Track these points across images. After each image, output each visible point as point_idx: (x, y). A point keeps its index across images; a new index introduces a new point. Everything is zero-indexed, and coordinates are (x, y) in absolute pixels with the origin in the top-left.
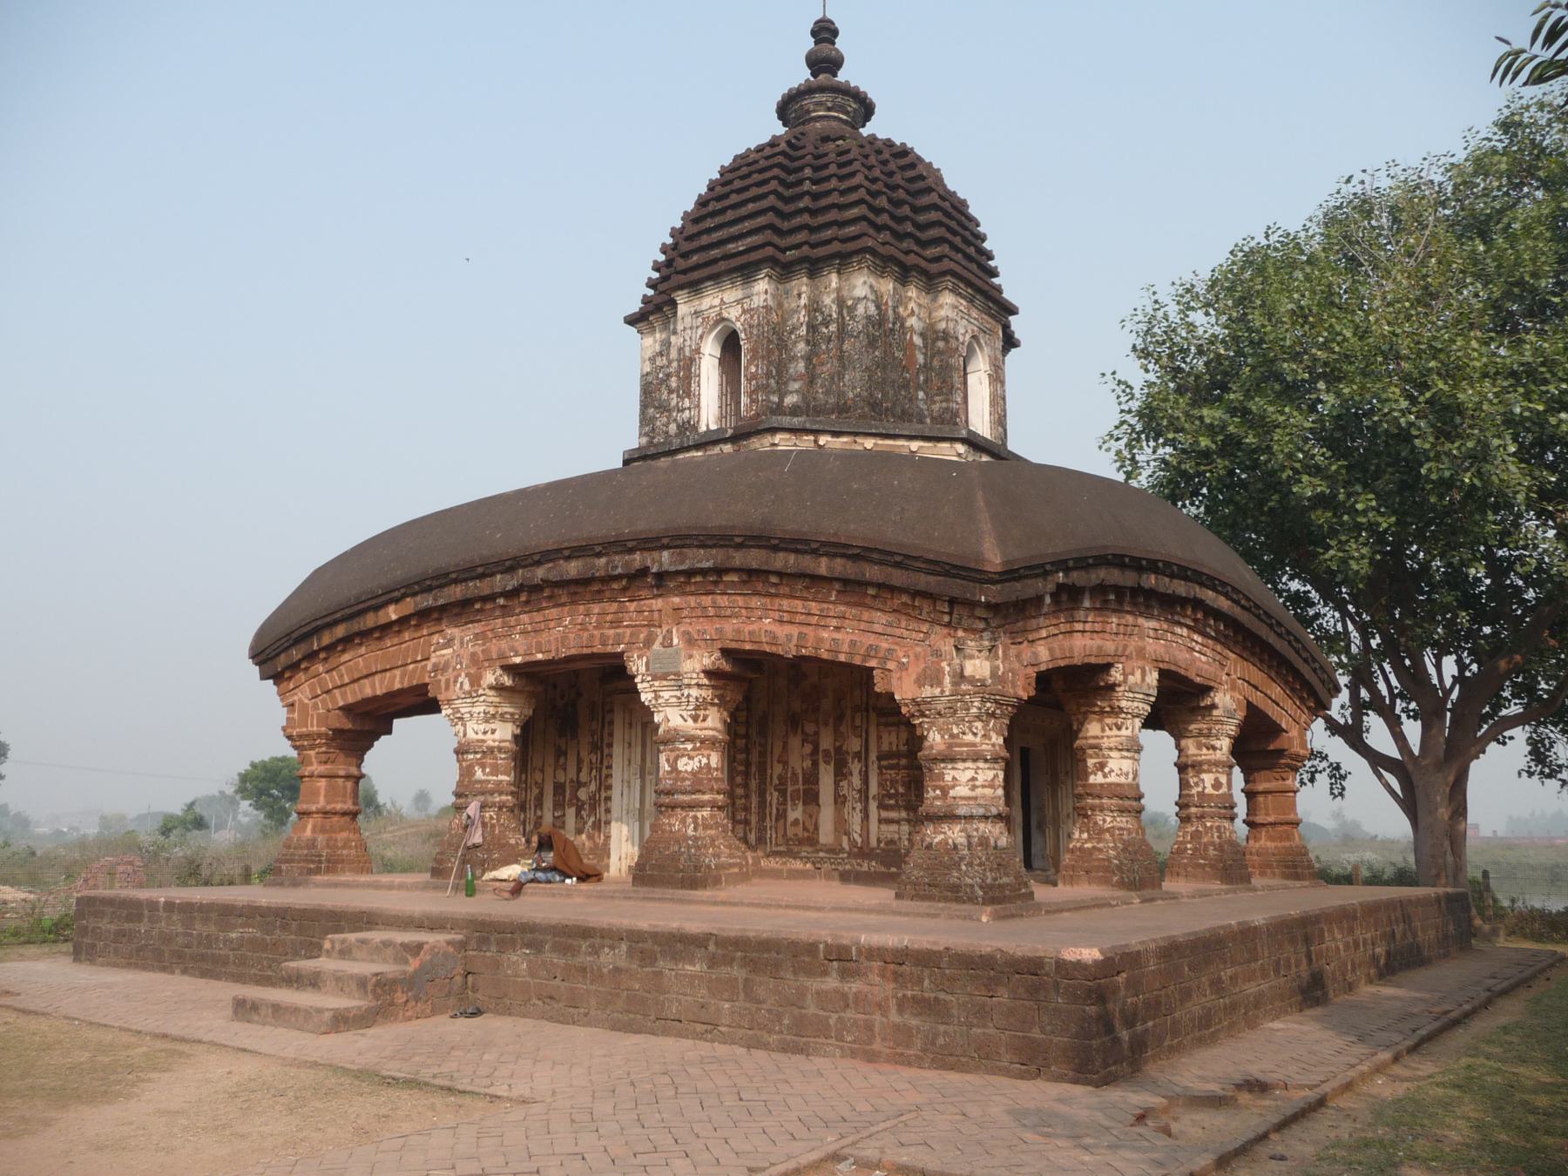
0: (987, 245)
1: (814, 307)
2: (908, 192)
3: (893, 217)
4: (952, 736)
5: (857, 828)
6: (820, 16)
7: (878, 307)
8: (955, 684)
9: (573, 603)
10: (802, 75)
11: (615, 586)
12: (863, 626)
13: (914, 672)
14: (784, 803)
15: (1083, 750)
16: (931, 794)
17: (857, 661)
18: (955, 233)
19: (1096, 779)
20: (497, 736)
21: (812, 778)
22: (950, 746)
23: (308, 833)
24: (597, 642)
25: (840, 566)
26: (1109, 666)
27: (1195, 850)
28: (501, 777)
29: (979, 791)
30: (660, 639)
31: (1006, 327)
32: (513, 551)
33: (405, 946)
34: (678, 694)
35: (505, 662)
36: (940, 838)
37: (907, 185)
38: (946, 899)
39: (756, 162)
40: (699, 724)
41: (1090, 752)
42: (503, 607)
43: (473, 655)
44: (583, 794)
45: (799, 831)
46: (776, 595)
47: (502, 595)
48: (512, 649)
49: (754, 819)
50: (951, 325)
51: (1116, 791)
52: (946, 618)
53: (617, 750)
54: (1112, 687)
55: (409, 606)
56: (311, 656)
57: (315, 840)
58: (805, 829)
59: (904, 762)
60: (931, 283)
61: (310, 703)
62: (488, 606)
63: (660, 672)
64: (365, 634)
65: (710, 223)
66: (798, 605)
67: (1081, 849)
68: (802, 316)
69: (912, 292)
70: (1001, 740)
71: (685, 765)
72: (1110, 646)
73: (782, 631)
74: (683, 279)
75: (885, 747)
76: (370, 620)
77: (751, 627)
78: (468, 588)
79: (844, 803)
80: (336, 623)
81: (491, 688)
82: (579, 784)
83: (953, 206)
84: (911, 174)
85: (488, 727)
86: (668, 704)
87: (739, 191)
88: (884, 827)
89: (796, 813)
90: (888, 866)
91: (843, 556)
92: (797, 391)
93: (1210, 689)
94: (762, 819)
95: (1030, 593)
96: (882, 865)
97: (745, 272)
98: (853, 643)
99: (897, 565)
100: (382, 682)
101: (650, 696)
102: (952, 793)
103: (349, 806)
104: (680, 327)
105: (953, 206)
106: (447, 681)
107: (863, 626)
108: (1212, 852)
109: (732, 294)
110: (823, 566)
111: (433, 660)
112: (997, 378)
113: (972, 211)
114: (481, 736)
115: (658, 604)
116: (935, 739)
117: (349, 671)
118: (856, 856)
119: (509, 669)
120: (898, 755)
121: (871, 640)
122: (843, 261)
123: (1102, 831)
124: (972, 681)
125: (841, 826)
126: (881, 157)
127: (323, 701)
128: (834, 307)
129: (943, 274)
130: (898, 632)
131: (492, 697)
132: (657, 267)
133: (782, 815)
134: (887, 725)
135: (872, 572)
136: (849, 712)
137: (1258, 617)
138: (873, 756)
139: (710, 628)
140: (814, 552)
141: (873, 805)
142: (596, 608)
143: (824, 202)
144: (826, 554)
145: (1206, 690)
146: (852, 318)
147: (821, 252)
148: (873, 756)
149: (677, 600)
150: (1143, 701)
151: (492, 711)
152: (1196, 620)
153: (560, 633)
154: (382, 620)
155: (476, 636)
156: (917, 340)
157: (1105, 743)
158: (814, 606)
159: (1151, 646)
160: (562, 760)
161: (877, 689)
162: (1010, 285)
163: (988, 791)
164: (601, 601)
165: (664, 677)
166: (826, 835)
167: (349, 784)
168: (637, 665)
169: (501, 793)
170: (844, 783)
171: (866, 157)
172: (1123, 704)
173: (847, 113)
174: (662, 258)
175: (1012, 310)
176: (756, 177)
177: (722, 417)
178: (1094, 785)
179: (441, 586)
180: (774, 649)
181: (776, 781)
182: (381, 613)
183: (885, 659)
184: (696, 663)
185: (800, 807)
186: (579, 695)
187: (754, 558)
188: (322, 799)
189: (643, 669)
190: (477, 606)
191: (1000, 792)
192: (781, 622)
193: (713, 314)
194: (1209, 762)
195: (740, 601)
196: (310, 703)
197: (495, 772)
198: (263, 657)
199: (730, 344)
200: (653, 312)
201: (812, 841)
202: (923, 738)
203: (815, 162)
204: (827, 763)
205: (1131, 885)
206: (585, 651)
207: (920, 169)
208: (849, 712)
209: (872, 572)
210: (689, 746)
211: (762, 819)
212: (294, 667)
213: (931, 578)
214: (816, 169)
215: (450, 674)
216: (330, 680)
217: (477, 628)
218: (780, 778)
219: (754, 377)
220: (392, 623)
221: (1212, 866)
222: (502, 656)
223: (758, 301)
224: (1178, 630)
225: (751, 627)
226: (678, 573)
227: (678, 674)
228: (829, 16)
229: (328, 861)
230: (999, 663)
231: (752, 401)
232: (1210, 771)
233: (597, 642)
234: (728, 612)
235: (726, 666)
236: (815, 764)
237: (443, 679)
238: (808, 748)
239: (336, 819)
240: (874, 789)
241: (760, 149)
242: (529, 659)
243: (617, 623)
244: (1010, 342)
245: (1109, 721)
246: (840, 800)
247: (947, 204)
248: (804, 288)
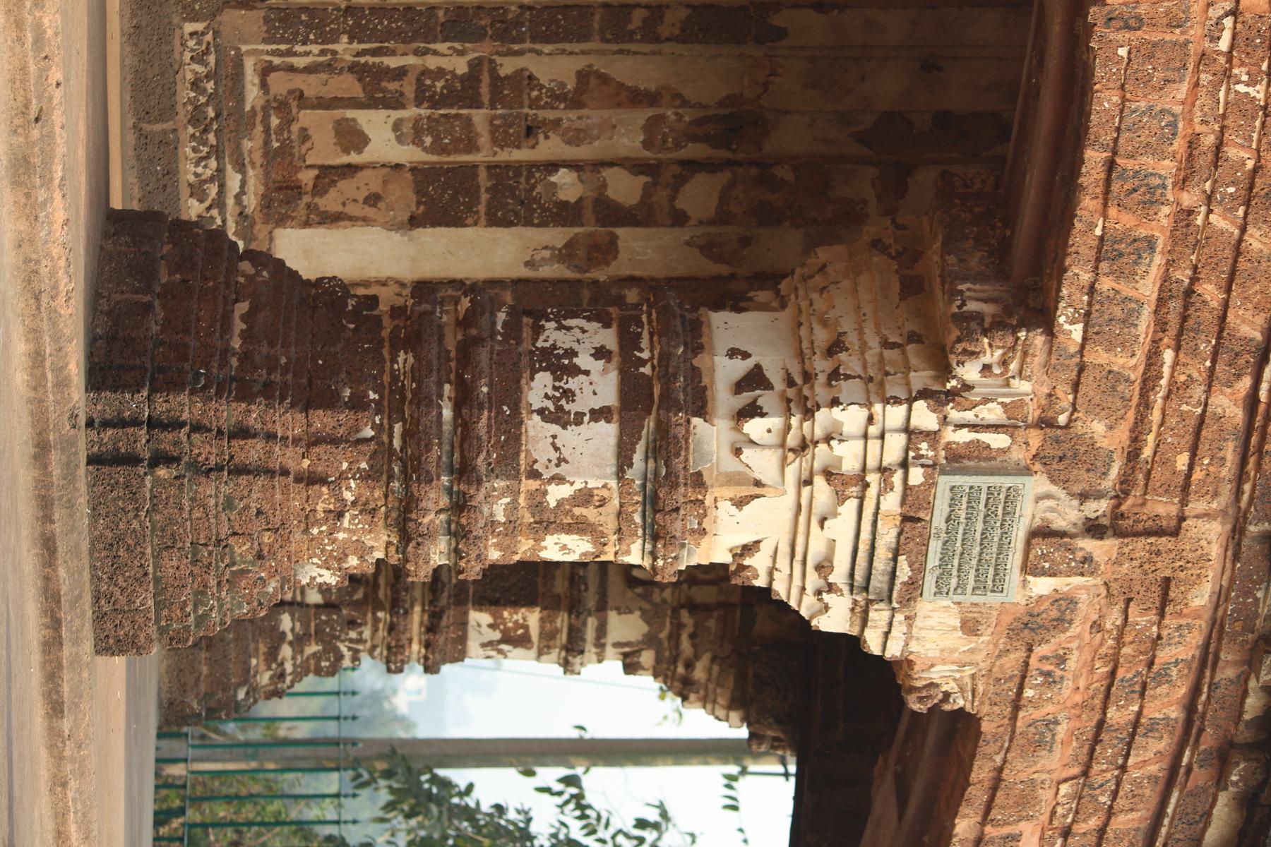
21: (512, 199)
30: (1067, 514)
34: (839, 576)
41: (562, 621)
58: (329, 175)
89: (383, 138)
101: (848, 456)
115: (1209, 535)
133: (377, 89)
139: (1061, 704)
149: (1201, 597)
178: (463, 624)
181: (507, 66)
185: (409, 154)
201: (286, 199)
204: (565, 254)
206: (1094, 158)
218: (524, 80)
234: (1103, 772)
236: (565, 214)
238: (624, 188)
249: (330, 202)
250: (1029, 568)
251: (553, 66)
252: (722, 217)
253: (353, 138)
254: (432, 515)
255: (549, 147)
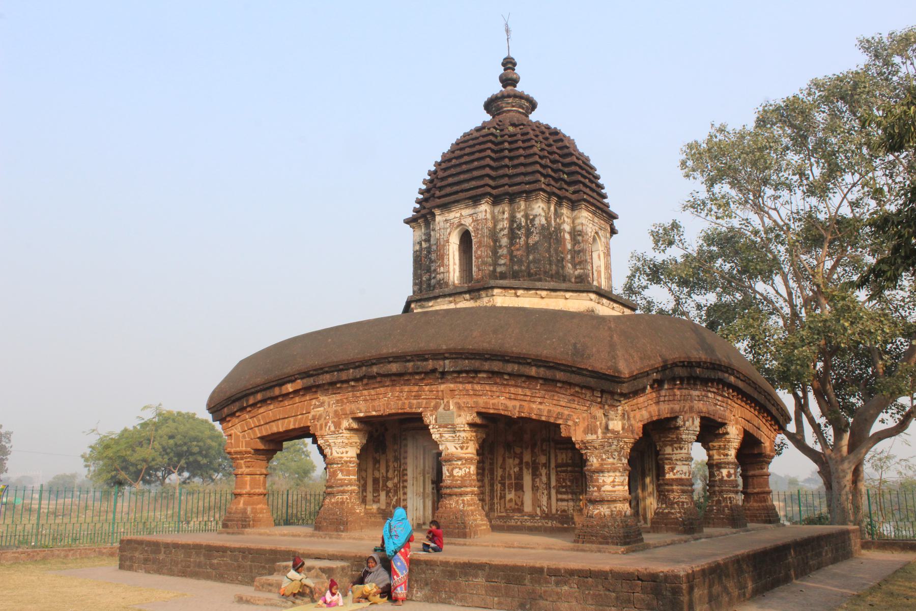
0: (600, 181)
1: (512, 219)
2: (560, 156)
3: (553, 170)
4: (602, 460)
5: (545, 503)
6: (506, 56)
7: (546, 219)
8: (603, 433)
9: (393, 385)
10: (497, 88)
11: (417, 377)
12: (555, 402)
13: (582, 426)
14: (504, 490)
15: (662, 459)
16: (592, 489)
17: (552, 420)
18: (585, 177)
19: (670, 476)
20: (349, 454)
21: (519, 477)
22: (602, 465)
23: (241, 505)
24: (407, 406)
25: (542, 372)
26: (676, 417)
27: (718, 510)
28: (351, 477)
29: (617, 488)
30: (442, 406)
31: (612, 226)
32: (360, 357)
33: (323, 570)
35: (353, 416)
36: (596, 512)
37: (558, 151)
38: (601, 543)
39: (477, 138)
40: (464, 451)
42: (353, 386)
43: (336, 412)
44: (390, 484)
45: (513, 504)
46: (507, 385)
47: (353, 380)
48: (358, 409)
49: (487, 498)
50: (584, 227)
51: (680, 482)
52: (599, 400)
53: (410, 461)
54: (678, 428)
55: (299, 384)
56: (242, 409)
57: (246, 509)
58: (516, 504)
59: (569, 469)
60: (574, 205)
61: (241, 435)
62: (345, 385)
63: (443, 424)
64: (274, 399)
65: (453, 171)
66: (520, 391)
67: (662, 513)
68: (506, 224)
69: (565, 211)
70: (626, 461)
71: (458, 473)
72: (677, 407)
73: (510, 404)
74: (438, 201)
75: (560, 461)
76: (277, 391)
77: (495, 401)
78: (333, 376)
79: (537, 490)
80: (257, 392)
81: (346, 429)
82: (387, 479)
83: (584, 162)
84: (560, 144)
85: (344, 450)
86: (447, 441)
87: (468, 154)
88: (560, 503)
90: (562, 523)
91: (545, 366)
92: (504, 264)
93: (725, 424)
94: (492, 498)
95: (641, 386)
96: (561, 524)
97: (476, 200)
98: (549, 411)
99: (573, 372)
100: (283, 425)
102: (603, 489)
103: (261, 490)
104: (437, 228)
105: (584, 162)
106: (321, 425)
107: (555, 402)
108: (726, 511)
109: (466, 212)
110: (533, 371)
111: (312, 413)
112: (608, 254)
113: (593, 162)
114: (340, 455)
115: (442, 387)
116: (594, 462)
117: (264, 418)
118: (544, 518)
119: (356, 419)
120: (567, 465)
121: (559, 409)
122: (529, 195)
123: (673, 503)
124: (613, 432)
125: (536, 503)
126: (544, 136)
127: (249, 434)
128: (523, 220)
129: (579, 201)
130: (574, 406)
131: (347, 434)
132: (421, 192)
133: (503, 497)
134: (560, 449)
135: (559, 375)
136: (539, 443)
137: (749, 384)
138: (553, 465)
139: (471, 401)
140: (529, 364)
141: (553, 492)
142: (406, 389)
143: (516, 162)
144: (535, 365)
145: (723, 425)
146: (533, 226)
147: (515, 189)
148: (553, 465)
149: (452, 386)
150: (694, 434)
151: (346, 441)
152: (718, 389)
153: (386, 401)
154: (284, 391)
155: (338, 401)
156: (567, 236)
157: (674, 457)
158: (528, 393)
159: (699, 405)
160: (377, 466)
161: (563, 435)
162: (613, 203)
163: (621, 488)
164: (409, 385)
165: (445, 426)
166: (528, 508)
167: (262, 477)
168: (429, 419)
169: (351, 485)
170: (537, 480)
171: (537, 136)
172: (684, 437)
173: (523, 108)
174: (424, 187)
175: (614, 217)
176: (478, 148)
177: (461, 277)
179: (318, 374)
180: (506, 413)
181: (499, 478)
182: (284, 387)
183: (567, 420)
184: (463, 419)
185: (513, 492)
186: (386, 430)
187: (496, 366)
188: (248, 487)
189: (433, 422)
190: (338, 385)
191: (627, 487)
192: (510, 399)
193: (456, 221)
194: (725, 463)
195: (488, 388)
196: (241, 435)
197: (348, 474)
198: (215, 409)
199: (466, 239)
200: (422, 217)
201: (520, 510)
202: (587, 460)
203: (509, 139)
204: (528, 469)
205: (686, 532)
206: (400, 411)
207: (571, 150)
208: (539, 443)
209: (559, 375)
210: (460, 463)
211: (492, 498)
212: (233, 415)
213: (591, 380)
214: (510, 143)
215: (322, 421)
216: (252, 422)
217: (338, 397)
219: (480, 257)
220: (288, 394)
221: (727, 519)
222: (352, 413)
223: (481, 216)
224: (710, 395)
225: (495, 401)
226: (454, 372)
227: (453, 425)
228: (512, 55)
229: (254, 521)
230: (625, 422)
231: (479, 270)
232: (725, 468)
233: (407, 406)
234: (481, 393)
235: (478, 421)
236: (521, 469)
237: (319, 424)
238: (517, 461)
239: (256, 497)
240: (553, 483)
241: (478, 130)
242: (368, 414)
243: (417, 397)
244: (613, 232)
245: (676, 445)
246: (535, 488)
247: (580, 162)
248: (506, 209)
249: (519, 503)
250: (449, 409)
251: (499, 473)
252: (521, 447)
253: (511, 500)
254: (448, 491)
255: (512, 472)
